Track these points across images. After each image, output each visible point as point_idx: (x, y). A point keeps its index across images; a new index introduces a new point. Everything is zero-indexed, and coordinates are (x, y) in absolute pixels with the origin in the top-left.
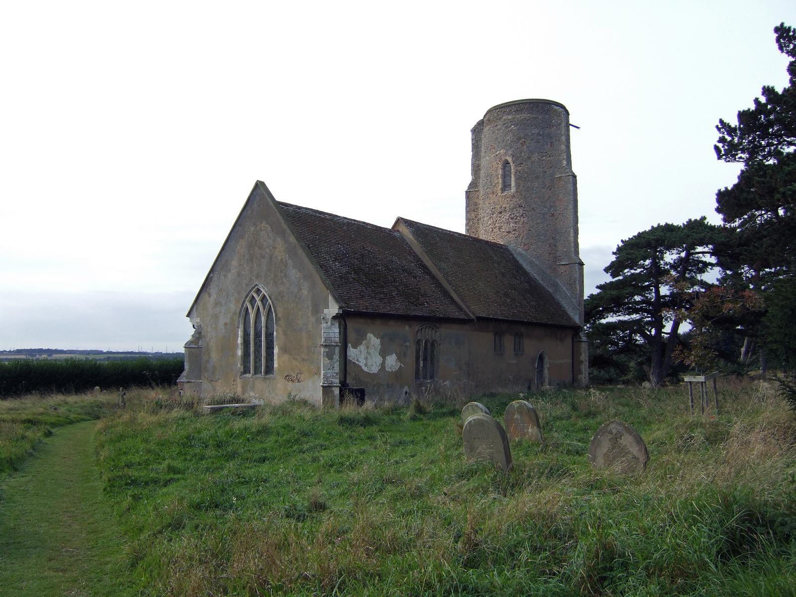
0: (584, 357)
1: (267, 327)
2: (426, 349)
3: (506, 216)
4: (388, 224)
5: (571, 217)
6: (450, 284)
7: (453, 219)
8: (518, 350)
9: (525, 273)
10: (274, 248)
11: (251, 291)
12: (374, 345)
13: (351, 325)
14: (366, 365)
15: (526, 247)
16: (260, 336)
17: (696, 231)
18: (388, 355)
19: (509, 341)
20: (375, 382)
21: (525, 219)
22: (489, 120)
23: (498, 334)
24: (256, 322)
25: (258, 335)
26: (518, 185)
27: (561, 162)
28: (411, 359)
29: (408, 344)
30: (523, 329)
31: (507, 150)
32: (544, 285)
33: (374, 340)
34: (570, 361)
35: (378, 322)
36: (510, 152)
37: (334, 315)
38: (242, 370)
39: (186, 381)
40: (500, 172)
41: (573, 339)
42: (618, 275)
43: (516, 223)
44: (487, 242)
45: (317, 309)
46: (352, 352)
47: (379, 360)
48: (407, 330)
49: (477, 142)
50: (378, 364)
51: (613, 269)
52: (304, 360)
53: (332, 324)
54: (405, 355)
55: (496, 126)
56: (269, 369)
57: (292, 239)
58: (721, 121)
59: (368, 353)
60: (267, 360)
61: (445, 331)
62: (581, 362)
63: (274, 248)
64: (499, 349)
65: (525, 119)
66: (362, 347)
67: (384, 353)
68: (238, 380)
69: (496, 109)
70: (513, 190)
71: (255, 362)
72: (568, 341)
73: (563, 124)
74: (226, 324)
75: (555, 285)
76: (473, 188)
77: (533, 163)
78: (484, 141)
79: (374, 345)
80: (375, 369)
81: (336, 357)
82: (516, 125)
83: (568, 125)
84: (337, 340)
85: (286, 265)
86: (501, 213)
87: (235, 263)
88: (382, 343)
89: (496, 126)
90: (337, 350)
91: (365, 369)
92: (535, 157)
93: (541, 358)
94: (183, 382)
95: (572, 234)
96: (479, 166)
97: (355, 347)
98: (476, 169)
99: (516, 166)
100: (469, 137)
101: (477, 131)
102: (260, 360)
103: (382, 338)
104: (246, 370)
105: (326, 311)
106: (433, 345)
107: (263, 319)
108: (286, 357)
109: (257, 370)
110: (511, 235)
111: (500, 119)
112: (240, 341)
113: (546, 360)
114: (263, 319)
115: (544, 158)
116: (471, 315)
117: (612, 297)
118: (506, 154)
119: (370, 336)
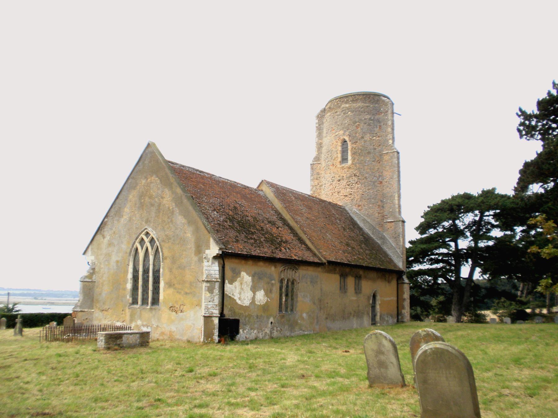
0: (406, 295)
1: (154, 265)
2: (287, 286)
3: (344, 183)
4: (254, 185)
5: (396, 185)
6: (305, 234)
7: (302, 185)
8: (358, 290)
9: (360, 229)
10: (162, 198)
11: (140, 234)
12: (246, 282)
13: (230, 264)
14: (240, 299)
15: (360, 208)
16: (148, 272)
17: (488, 200)
18: (258, 290)
19: (350, 281)
20: (247, 314)
21: (359, 186)
22: (330, 108)
23: (343, 276)
24: (144, 261)
25: (146, 271)
26: (353, 159)
27: (388, 141)
28: (275, 294)
29: (273, 282)
30: (361, 272)
31: (345, 131)
32: (374, 238)
33: (246, 278)
34: (395, 299)
35: (250, 262)
36: (347, 133)
37: (215, 255)
38: (131, 301)
39: (79, 310)
40: (340, 148)
41: (397, 281)
42: (425, 233)
43: (351, 188)
44: (330, 203)
45: (199, 250)
46: (228, 287)
47: (250, 294)
48: (273, 270)
49: (320, 125)
50: (249, 298)
51: (422, 228)
52: (186, 293)
53: (213, 263)
54: (271, 291)
56: (156, 301)
57: (179, 191)
58: (520, 110)
59: (242, 289)
60: (153, 293)
61: (303, 272)
62: (404, 300)
63: (162, 198)
64: (343, 289)
65: (359, 107)
66: (237, 283)
67: (254, 289)
68: (127, 310)
70: (350, 162)
71: (143, 295)
72: (394, 283)
73: (390, 112)
74: (117, 262)
75: (383, 238)
76: (316, 161)
77: (365, 141)
78: (326, 125)
79: (246, 282)
80: (247, 303)
81: (217, 291)
82: (352, 112)
83: (393, 113)
84: (218, 276)
85: (173, 213)
86: (339, 181)
87: (127, 210)
88: (253, 281)
89: (336, 112)
90: (217, 285)
91: (239, 302)
92: (367, 137)
93: (374, 296)
94: (77, 311)
95: (396, 198)
96: (321, 144)
97: (231, 283)
98: (320, 146)
99: (352, 144)
100: (314, 122)
101: (321, 116)
102: (148, 293)
103: (253, 276)
104: (135, 302)
105: (207, 252)
106: (293, 283)
107: (151, 258)
108: (170, 291)
110: (347, 198)
111: (339, 107)
112: (130, 276)
113: (378, 298)
114: (151, 258)
115: (374, 138)
116: (323, 259)
117: (419, 252)
119: (243, 274)
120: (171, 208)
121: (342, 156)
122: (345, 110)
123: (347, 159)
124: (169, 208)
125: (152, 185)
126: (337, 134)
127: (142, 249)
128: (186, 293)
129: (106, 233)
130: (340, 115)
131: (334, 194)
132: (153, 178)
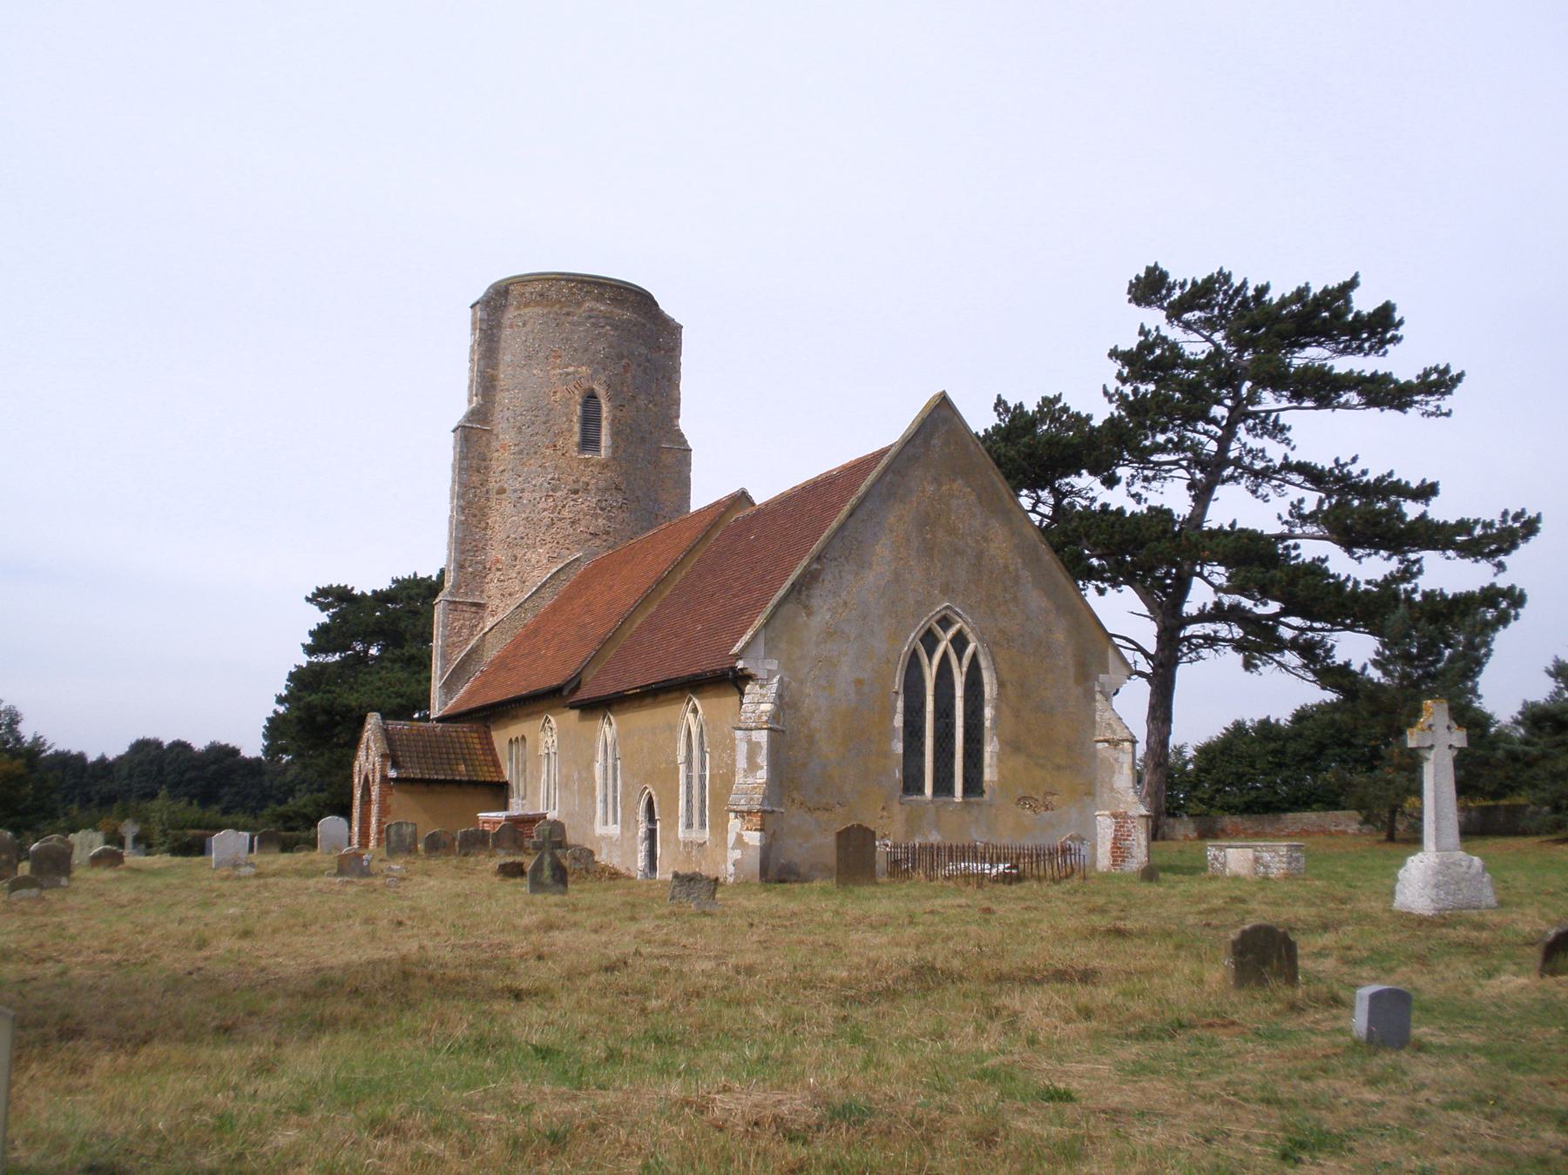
26: (615, 447)
52: (1059, 767)
55: (568, 314)
56: (973, 783)
63: (986, 539)
65: (629, 321)
68: (896, 808)
69: (568, 280)
74: (859, 683)
76: (478, 422)
77: (638, 409)
82: (615, 327)
85: (1017, 580)
89: (568, 314)
92: (642, 401)
98: (486, 384)
109: (943, 784)
111: (579, 304)
118: (592, 378)
120: (1012, 568)
121: (584, 431)
122: (597, 317)
123: (597, 443)
124: (1006, 567)
125: (954, 502)
126: (571, 369)
127: (960, 659)
128: (1059, 767)
129: (815, 602)
130: (580, 324)
131: (560, 524)
132: (955, 486)
